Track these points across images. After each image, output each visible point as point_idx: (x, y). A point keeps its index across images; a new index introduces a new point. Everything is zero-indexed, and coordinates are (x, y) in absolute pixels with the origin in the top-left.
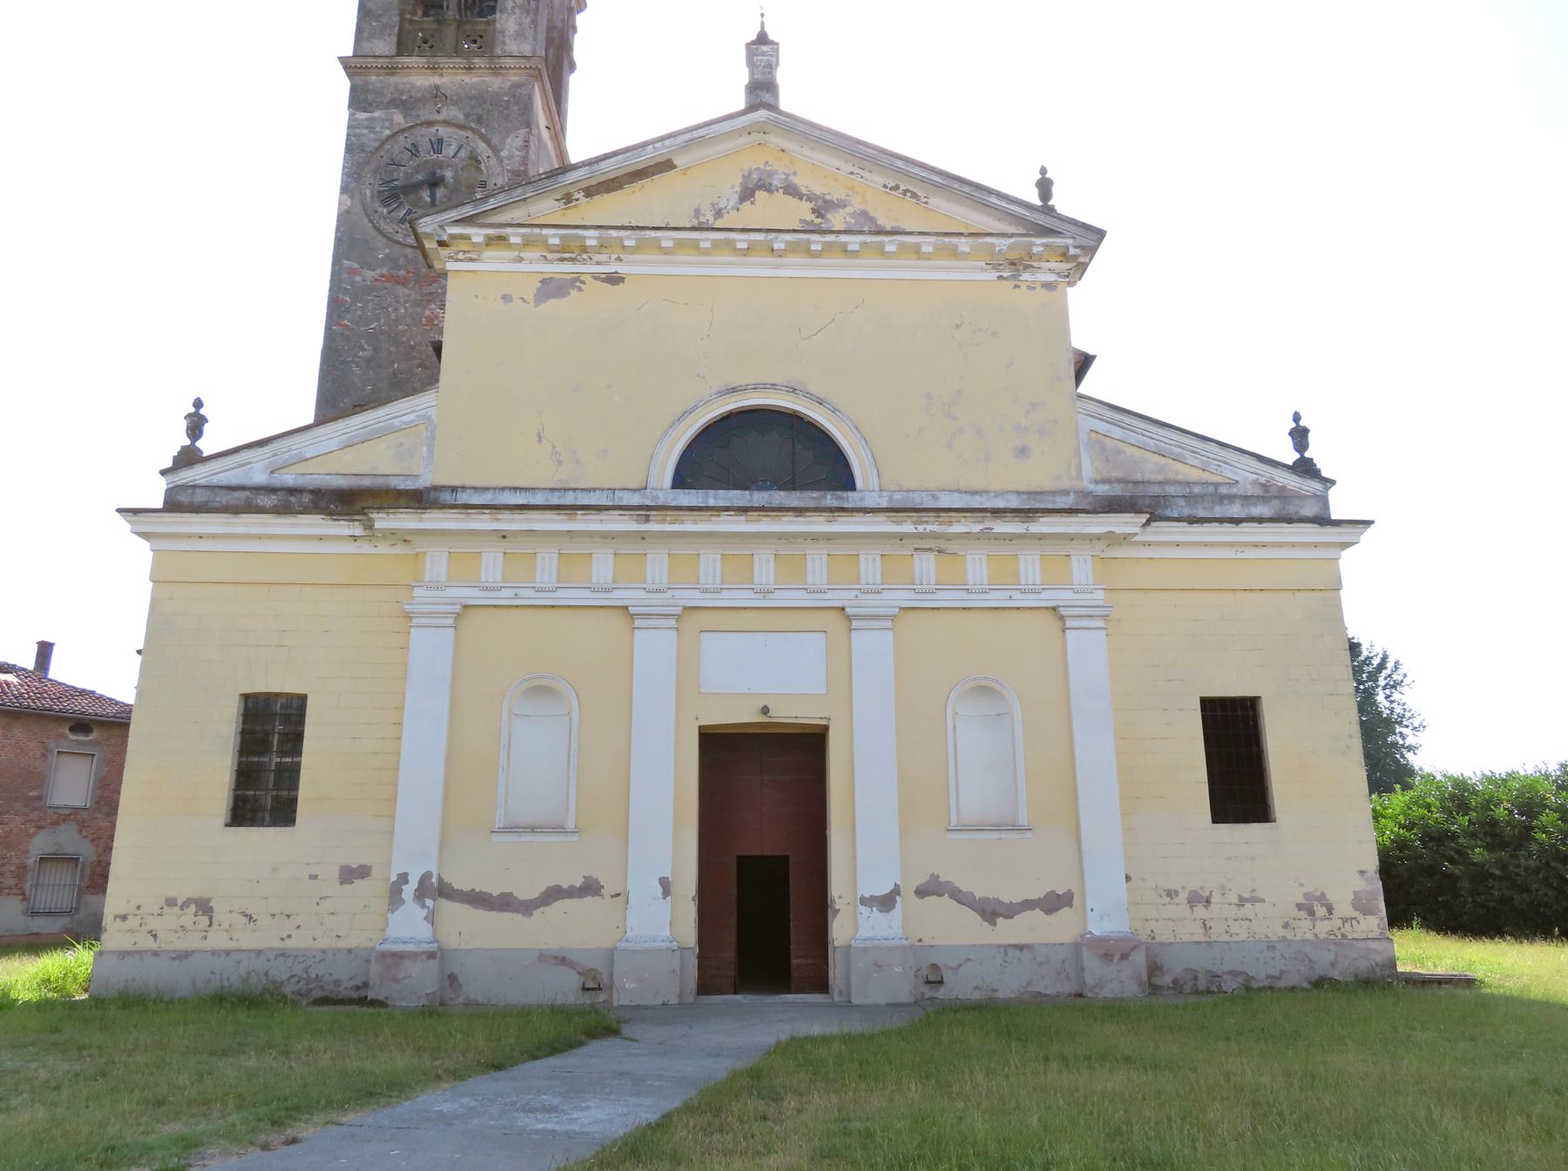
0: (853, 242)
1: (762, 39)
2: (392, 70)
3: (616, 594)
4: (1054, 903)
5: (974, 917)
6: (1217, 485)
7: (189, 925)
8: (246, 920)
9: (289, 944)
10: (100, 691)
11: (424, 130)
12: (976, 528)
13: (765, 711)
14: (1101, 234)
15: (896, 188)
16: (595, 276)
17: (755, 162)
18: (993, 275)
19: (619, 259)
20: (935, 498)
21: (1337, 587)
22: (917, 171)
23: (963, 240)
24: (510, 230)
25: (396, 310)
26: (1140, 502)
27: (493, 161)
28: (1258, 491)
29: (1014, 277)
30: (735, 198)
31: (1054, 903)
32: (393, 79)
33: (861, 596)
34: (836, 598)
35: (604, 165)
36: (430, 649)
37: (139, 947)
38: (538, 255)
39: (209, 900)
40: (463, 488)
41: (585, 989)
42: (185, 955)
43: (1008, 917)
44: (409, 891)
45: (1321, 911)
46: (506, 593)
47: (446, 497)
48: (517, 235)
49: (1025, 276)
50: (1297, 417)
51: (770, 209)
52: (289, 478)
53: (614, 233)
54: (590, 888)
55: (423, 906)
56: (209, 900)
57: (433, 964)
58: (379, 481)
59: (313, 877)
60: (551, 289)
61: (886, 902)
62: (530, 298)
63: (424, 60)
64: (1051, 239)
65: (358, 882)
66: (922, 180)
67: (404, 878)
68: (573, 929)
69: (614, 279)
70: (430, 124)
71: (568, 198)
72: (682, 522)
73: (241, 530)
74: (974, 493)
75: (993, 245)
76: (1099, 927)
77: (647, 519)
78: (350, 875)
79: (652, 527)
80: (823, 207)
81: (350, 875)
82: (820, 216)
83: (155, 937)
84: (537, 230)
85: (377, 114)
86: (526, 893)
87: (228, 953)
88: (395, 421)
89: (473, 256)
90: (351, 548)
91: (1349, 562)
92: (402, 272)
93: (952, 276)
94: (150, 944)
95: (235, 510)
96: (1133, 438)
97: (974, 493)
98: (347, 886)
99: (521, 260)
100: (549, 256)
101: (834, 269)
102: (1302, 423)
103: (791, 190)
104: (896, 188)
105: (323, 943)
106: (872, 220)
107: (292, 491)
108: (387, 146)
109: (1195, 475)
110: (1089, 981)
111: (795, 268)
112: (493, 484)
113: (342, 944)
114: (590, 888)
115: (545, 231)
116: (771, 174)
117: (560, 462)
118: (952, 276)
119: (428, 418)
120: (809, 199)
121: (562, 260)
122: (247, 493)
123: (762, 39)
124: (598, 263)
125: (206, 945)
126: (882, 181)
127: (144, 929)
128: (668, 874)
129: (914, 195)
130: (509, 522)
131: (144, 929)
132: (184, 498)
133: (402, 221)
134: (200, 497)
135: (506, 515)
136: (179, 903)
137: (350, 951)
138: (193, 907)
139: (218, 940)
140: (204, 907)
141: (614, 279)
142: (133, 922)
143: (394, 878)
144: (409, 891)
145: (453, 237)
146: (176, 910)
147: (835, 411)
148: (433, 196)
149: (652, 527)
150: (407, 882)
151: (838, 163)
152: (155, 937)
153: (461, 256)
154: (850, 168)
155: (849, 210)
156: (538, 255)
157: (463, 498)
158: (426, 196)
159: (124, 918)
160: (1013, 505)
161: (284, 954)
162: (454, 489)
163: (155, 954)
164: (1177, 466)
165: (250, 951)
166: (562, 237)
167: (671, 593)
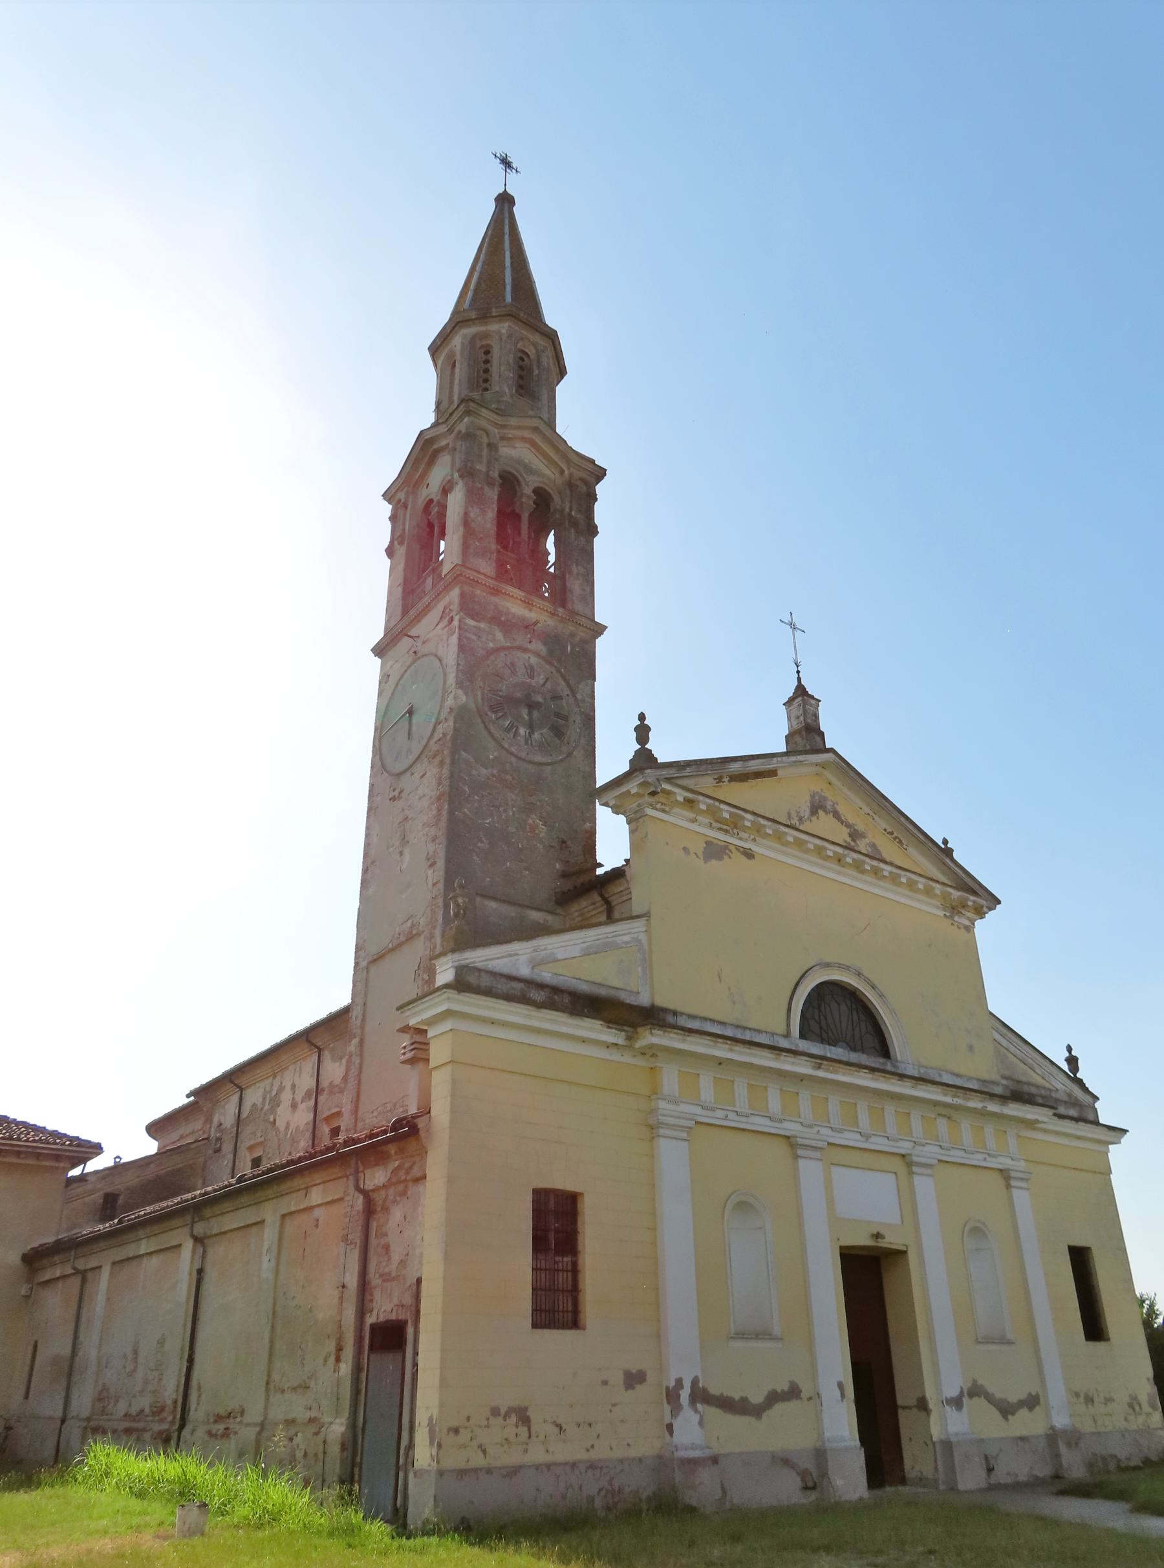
0: (869, 863)
1: (801, 690)
2: (496, 592)
3: (786, 1125)
4: (1032, 1402)
5: (996, 1414)
6: (1050, 1090)
7: (512, 1438)
8: (222, 1412)
9: (594, 1455)
10: (12, 1115)
11: (519, 654)
12: (979, 1105)
13: (877, 1236)
14: (999, 902)
15: (892, 833)
16: (738, 848)
17: (817, 786)
18: (941, 913)
19: (754, 840)
20: (940, 1075)
21: (1109, 1172)
22: (911, 827)
23: (938, 886)
24: (701, 798)
25: (505, 811)
26: (1019, 1095)
27: (571, 700)
28: (1066, 1099)
29: (952, 917)
30: (807, 814)
31: (1032, 1402)
32: (495, 599)
33: (988, 1159)
34: (905, 1147)
35: (752, 763)
36: (673, 1156)
37: (473, 1464)
38: (707, 821)
39: (526, 1409)
40: (682, 1014)
41: (806, 1488)
42: (514, 1471)
43: (1013, 1414)
44: (685, 1394)
45: (1137, 1408)
46: (719, 1114)
47: (670, 1019)
48: (704, 803)
49: (956, 918)
50: (1069, 1049)
51: (824, 824)
52: (546, 975)
53: (763, 822)
54: (793, 1392)
55: (696, 1411)
56: (526, 1409)
57: (49, 1451)
58: (612, 993)
59: (605, 1383)
60: (714, 852)
61: (957, 1403)
62: (700, 854)
63: (522, 594)
64: (972, 897)
65: (638, 1387)
66: (913, 835)
67: (679, 1383)
68: (783, 1431)
69: (749, 854)
70: (526, 650)
71: (720, 780)
72: (836, 1072)
73: (535, 1023)
74: (958, 1075)
75: (950, 894)
76: (1061, 1421)
77: (819, 1067)
78: (634, 1379)
79: (821, 1074)
80: (855, 835)
81: (634, 1379)
82: (853, 840)
83: (484, 1452)
84: (717, 804)
85: (482, 625)
86: (757, 1398)
87: (549, 1466)
88: (618, 939)
89: (667, 809)
90: (603, 1054)
91: (1115, 1153)
92: (509, 777)
93: (924, 907)
94: (479, 1461)
95: (508, 998)
96: (1012, 1049)
97: (958, 1075)
98: (630, 1392)
99: (694, 821)
100: (714, 824)
101: (848, 878)
102: (1073, 1053)
103: (836, 815)
104: (892, 833)
105: (618, 1453)
106: (878, 851)
107: (555, 990)
108: (492, 658)
109: (1039, 1080)
110: (1065, 1464)
111: (829, 872)
112: (711, 1016)
113: (634, 1453)
114: (793, 1392)
115: (722, 806)
116: (825, 799)
117: (734, 1003)
118: (924, 907)
119: (639, 941)
120: (848, 826)
121: (720, 829)
122: (522, 985)
123: (801, 690)
124: (740, 839)
125: (529, 1459)
126: (884, 825)
127: (475, 1443)
128: (842, 1379)
129: (900, 842)
130: (722, 1051)
131: (475, 1443)
132: (472, 979)
133: (508, 729)
134: (486, 981)
135: (739, 1048)
136: (503, 1412)
137: (640, 1460)
138: (513, 1419)
139: (536, 1455)
140: (523, 1417)
141: (749, 854)
142: (464, 1436)
143: (672, 1384)
144: (685, 1394)
145: (664, 791)
146: (501, 1418)
147: (881, 996)
148: (530, 714)
149: (821, 1074)
150: (682, 1387)
151: (862, 805)
152: (484, 1452)
153: (659, 806)
154: (867, 810)
155: (867, 841)
156: (707, 821)
157: (682, 1021)
158: (525, 712)
159: (456, 1431)
160: (976, 1087)
161: (592, 1466)
162: (675, 1013)
163: (489, 1471)
164: (1032, 1073)
165: (566, 1464)
166: (731, 814)
167: (816, 1129)
